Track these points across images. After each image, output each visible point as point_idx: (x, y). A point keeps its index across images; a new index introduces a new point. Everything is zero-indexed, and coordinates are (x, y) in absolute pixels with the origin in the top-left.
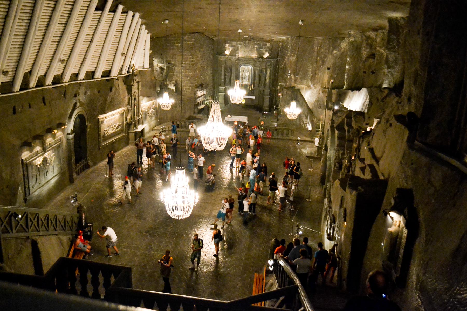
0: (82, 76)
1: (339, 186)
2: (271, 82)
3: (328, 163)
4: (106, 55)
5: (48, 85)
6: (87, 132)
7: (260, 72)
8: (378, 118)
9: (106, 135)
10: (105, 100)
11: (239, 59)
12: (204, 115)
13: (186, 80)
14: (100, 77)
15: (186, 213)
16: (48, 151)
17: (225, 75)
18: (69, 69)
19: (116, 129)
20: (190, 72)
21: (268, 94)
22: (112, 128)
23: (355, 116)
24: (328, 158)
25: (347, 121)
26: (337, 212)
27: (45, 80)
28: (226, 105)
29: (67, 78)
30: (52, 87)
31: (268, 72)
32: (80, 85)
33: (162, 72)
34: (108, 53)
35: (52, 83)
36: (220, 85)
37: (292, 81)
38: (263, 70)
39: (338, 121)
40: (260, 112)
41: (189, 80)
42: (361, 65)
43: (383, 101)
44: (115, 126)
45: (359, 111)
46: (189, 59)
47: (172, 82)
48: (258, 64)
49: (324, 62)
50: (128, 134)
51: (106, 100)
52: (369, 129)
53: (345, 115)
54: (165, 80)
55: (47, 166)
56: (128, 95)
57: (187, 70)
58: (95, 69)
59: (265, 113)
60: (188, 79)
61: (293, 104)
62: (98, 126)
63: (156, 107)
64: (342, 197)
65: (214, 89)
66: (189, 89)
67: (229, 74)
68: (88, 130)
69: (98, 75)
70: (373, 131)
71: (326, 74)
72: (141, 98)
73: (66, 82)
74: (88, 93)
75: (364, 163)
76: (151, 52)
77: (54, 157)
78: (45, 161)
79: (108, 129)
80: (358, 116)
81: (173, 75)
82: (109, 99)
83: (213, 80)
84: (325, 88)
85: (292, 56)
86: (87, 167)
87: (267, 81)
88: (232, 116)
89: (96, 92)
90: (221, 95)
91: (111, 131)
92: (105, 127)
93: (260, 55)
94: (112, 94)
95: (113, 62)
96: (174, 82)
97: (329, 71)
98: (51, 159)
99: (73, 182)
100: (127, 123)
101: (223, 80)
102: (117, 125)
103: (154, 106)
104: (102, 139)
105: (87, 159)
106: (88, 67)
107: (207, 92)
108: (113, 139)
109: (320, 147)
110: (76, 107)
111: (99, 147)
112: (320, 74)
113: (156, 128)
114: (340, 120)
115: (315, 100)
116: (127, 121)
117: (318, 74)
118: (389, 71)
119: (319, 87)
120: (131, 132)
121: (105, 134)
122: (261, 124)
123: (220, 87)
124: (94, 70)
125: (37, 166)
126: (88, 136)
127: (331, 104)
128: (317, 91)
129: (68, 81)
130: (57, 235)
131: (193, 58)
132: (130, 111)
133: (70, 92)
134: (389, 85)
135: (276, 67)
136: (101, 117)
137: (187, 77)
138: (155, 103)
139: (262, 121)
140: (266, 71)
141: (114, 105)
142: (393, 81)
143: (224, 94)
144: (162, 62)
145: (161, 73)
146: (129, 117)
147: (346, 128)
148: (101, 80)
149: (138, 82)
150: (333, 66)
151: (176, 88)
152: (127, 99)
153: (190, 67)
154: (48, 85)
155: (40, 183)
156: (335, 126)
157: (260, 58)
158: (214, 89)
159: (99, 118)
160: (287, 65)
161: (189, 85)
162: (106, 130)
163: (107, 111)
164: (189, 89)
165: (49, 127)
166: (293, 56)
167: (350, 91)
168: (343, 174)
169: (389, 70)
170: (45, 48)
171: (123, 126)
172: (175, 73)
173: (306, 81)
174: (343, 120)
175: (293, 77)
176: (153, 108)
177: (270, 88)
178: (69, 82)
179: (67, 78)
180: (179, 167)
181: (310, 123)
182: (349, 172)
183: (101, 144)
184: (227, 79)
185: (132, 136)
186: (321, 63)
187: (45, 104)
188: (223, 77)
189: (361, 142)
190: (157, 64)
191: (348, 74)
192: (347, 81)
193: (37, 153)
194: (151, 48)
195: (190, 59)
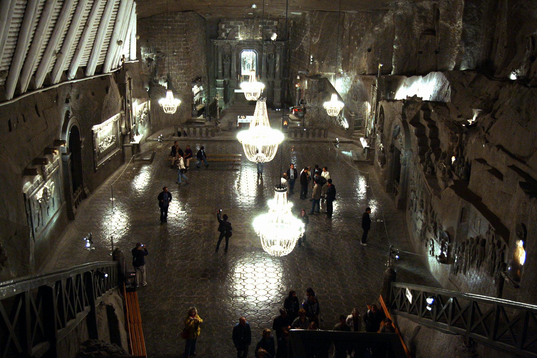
0: (73, 73)
1: (456, 195)
2: (282, 70)
3: (402, 167)
4: (101, 46)
5: (39, 89)
6: (82, 150)
7: (268, 58)
8: (479, 108)
9: (101, 152)
10: (102, 105)
11: (240, 43)
12: (205, 118)
13: (181, 74)
14: (93, 74)
15: (284, 248)
16: (48, 179)
17: (223, 65)
18: (62, 66)
19: (110, 143)
20: (185, 63)
21: (280, 85)
22: (106, 141)
23: (434, 108)
24: (402, 162)
25: (424, 114)
26: (455, 229)
27: (35, 82)
28: (226, 103)
29: (58, 78)
30: (43, 92)
31: (278, 59)
32: (72, 86)
33: (149, 64)
34: (104, 41)
35: (43, 85)
36: (217, 78)
37: (315, 67)
38: (271, 55)
39: (410, 114)
40: (272, 110)
41: (184, 74)
42: (413, 44)
43: (472, 87)
44: (109, 139)
45: (428, 99)
46: (182, 46)
47: (163, 77)
48: (265, 48)
49: (359, 42)
50: (123, 147)
51: (102, 105)
52: (470, 121)
53: (419, 107)
54: (154, 73)
55: (48, 200)
56: (121, 97)
57: (181, 60)
58: (87, 64)
59: (277, 110)
60: (183, 71)
61: (334, 96)
62: (93, 140)
63: (148, 111)
64: (463, 208)
65: (209, 84)
66: (184, 84)
67: (229, 63)
68: (82, 147)
69: (91, 71)
70: (478, 125)
71: (364, 57)
72: (133, 99)
73: (56, 84)
74: (81, 96)
75: (488, 165)
76: (139, 38)
77: (54, 187)
78: (45, 193)
79: (102, 144)
80: (439, 107)
81: (164, 67)
82: (105, 104)
83: (208, 71)
84: (364, 74)
85: (315, 36)
86: (84, 196)
87: (277, 69)
88: (247, 116)
89: (90, 94)
90: (218, 90)
91: (106, 146)
92: (99, 141)
93: (267, 37)
94: (108, 97)
95: (106, 54)
96: (166, 77)
97: (371, 53)
98: (51, 190)
99: (74, 219)
100: (122, 133)
101: (220, 72)
102: (111, 138)
103: (146, 109)
104: (97, 157)
105: (83, 186)
106: (80, 62)
107: (203, 87)
108: (108, 157)
109: (371, 148)
110: (69, 117)
111: (95, 168)
112: (355, 57)
113: (149, 138)
114: (414, 113)
115: (348, 90)
116: (121, 131)
117: (352, 58)
118: (468, 50)
119: (354, 74)
120: (126, 146)
121: (100, 151)
122: (284, 124)
123: (217, 80)
124: (85, 65)
125: (38, 201)
126: (83, 155)
127: (383, 94)
128: (351, 79)
129: (58, 82)
130: (111, 294)
131: (188, 45)
132: (123, 118)
133: (63, 97)
134: (469, 66)
135: (287, 51)
136: (95, 128)
137: (182, 70)
138: (146, 105)
139: (285, 120)
140: (275, 57)
141: (109, 112)
142: (474, 61)
143: (223, 88)
144: (148, 51)
145: (148, 66)
146: (123, 126)
147: (424, 123)
148: (94, 78)
149: (129, 79)
150: (375, 47)
151: (168, 85)
152: (120, 101)
153: (184, 55)
154: (39, 89)
155: (43, 225)
156: (408, 121)
157: (267, 40)
158: (209, 84)
159: (93, 129)
160: (305, 48)
161: (184, 80)
162: (101, 146)
163: (102, 120)
164: (184, 84)
165: (45, 146)
166: (316, 36)
167: (405, 77)
168: (443, 180)
169: (468, 48)
170: (42, 36)
171: (117, 139)
172: (166, 65)
173: (334, 67)
174: (418, 114)
175: (317, 63)
176: (145, 113)
177: (280, 78)
178: (60, 83)
179: (58, 78)
180: (281, 189)
181: (345, 119)
182: (451, 176)
183: (97, 165)
184: (225, 70)
185: (128, 151)
186: (356, 43)
187: (39, 116)
188: (220, 67)
189: (464, 139)
190: (145, 55)
191: (396, 56)
192: (395, 65)
193: (38, 183)
194: (137, 34)
195: (184, 45)
